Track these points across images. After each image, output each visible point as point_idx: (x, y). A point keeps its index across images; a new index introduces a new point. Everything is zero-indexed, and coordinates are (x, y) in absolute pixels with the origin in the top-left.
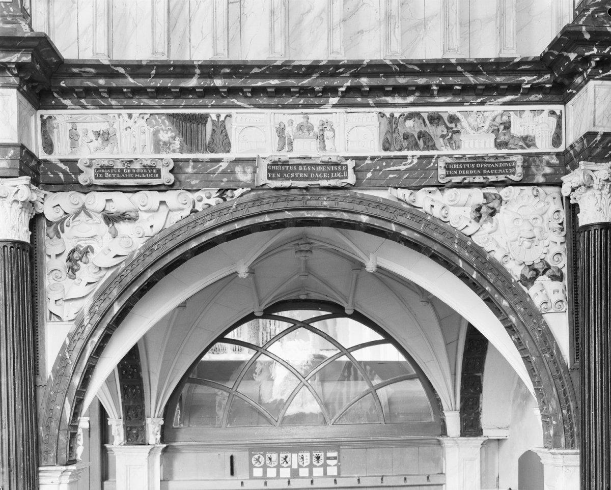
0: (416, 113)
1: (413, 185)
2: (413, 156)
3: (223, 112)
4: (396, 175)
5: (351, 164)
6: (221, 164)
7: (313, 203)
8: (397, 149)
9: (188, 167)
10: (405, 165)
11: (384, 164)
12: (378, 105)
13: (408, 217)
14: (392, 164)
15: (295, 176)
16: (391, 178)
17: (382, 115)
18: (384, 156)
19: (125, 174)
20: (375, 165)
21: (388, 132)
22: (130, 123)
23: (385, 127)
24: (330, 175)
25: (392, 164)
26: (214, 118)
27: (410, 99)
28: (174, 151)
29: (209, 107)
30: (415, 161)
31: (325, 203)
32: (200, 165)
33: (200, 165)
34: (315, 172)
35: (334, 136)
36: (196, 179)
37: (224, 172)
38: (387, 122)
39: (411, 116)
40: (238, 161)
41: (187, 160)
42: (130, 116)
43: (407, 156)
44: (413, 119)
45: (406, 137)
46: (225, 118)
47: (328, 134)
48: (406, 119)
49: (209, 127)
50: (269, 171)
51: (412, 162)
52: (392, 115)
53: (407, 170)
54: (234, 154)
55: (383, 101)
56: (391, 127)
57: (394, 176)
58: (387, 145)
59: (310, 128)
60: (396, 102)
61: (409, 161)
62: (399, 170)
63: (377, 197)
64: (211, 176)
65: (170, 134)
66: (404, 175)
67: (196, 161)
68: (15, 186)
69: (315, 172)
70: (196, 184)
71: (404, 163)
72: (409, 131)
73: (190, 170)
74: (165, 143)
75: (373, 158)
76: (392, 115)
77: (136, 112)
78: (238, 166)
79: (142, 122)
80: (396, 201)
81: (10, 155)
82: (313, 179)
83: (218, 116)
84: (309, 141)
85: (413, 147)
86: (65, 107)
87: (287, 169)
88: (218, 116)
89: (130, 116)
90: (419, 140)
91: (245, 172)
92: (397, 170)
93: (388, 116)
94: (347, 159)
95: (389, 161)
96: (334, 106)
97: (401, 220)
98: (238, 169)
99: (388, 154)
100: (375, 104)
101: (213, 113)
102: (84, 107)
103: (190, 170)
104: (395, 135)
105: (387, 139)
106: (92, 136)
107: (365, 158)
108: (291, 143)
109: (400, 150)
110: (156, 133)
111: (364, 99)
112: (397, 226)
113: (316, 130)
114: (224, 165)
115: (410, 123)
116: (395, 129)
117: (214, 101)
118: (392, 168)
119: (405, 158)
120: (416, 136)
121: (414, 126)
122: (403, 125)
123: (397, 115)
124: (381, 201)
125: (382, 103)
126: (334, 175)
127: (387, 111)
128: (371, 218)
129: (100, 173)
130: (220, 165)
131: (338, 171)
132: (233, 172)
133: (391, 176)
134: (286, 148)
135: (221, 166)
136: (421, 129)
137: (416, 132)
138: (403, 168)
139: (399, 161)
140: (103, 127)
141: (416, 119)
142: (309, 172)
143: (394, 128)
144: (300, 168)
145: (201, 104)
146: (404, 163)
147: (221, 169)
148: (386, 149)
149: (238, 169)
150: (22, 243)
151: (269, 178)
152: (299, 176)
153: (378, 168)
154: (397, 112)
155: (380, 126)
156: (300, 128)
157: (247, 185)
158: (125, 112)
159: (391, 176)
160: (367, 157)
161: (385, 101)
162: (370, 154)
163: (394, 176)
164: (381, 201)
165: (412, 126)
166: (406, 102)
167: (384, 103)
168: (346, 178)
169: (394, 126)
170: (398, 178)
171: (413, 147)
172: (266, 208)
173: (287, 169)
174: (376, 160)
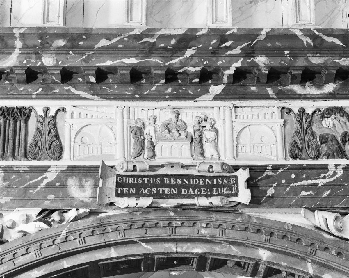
0: (337, 108)
1: (338, 206)
2: (336, 166)
3: (54, 105)
4: (311, 192)
5: (243, 175)
6: (45, 175)
7: (185, 232)
8: (312, 156)
10: (324, 178)
11: (293, 176)
12: (282, 96)
13: (333, 253)
14: (304, 176)
15: (158, 192)
16: (303, 196)
17: (285, 111)
18: (292, 165)
20: (281, 176)
21: (297, 133)
23: (293, 125)
24: (212, 191)
25: (304, 176)
26: (41, 113)
27: (329, 88)
29: (34, 96)
30: (340, 172)
31: (203, 231)
32: (14, 176)
33: (14, 176)
34: (188, 187)
35: (217, 138)
36: (7, 196)
37: (50, 186)
38: (295, 120)
39: (330, 111)
40: (73, 170)
43: (327, 165)
44: (333, 117)
45: (324, 139)
46: (57, 113)
47: (208, 135)
48: (323, 117)
49: (32, 124)
50: (118, 185)
51: (335, 173)
52: (302, 111)
53: (327, 185)
54: (67, 161)
55: (289, 90)
56: (301, 126)
57: (309, 193)
58: (297, 151)
59: (182, 128)
60: (308, 93)
61: (330, 173)
62: (316, 185)
63: (284, 223)
64: (31, 191)
66: (323, 192)
69: (188, 187)
70: (6, 203)
71: (323, 175)
72: (327, 131)
75: (275, 168)
76: (302, 111)
78: (72, 178)
80: (313, 229)
82: (184, 197)
83: (47, 109)
84: (177, 145)
85: (335, 154)
87: (146, 182)
90: (344, 144)
91: (81, 186)
92: (312, 185)
93: (297, 112)
94: (236, 168)
95: (300, 172)
96: (217, 98)
97: (322, 256)
98: (72, 182)
99: (298, 162)
100: (276, 95)
104: (307, 138)
105: (296, 143)
107: (264, 168)
108: (153, 146)
109: (317, 157)
111: (261, 87)
112: (316, 266)
113: (190, 130)
114: (51, 176)
115: (328, 122)
116: (307, 129)
117: (40, 89)
118: (305, 182)
119: (325, 168)
120: (339, 139)
121: (334, 126)
122: (319, 124)
123: (309, 111)
124: (290, 228)
125: (288, 93)
126: (217, 191)
127: (295, 105)
128: (275, 254)
130: (44, 176)
131: (223, 186)
132: (64, 186)
133: (304, 193)
134: (146, 154)
135: (46, 178)
136: (346, 130)
137: (338, 133)
138: (321, 182)
139: (315, 172)
141: (338, 117)
142: (179, 187)
143: (305, 128)
144: (166, 181)
145: (22, 93)
146: (323, 175)
147: (45, 182)
148: (294, 157)
149: (72, 182)
151: (118, 195)
152: (164, 192)
153: (283, 181)
154: (310, 106)
155: (284, 125)
156: (167, 127)
157: (85, 205)
159: (304, 193)
160: (268, 166)
161: (292, 90)
162: (271, 163)
163: (309, 193)
164: (290, 228)
165: (332, 125)
166: (322, 92)
167: (290, 93)
168: (236, 195)
169: (305, 125)
170: (315, 196)
171: (335, 154)
172: (112, 237)
173: (146, 182)
174: (281, 170)
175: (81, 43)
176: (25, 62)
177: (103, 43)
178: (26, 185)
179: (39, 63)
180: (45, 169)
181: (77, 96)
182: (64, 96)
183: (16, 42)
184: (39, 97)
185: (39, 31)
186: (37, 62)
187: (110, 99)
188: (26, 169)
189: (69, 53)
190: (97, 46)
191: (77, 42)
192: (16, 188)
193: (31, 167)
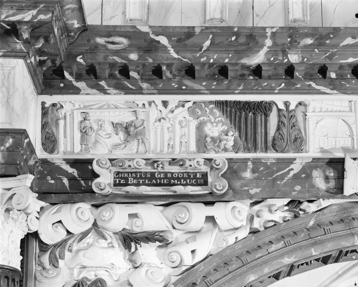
3: (294, 99)
6: (292, 166)
9: (245, 170)
19: (156, 179)
22: (165, 111)
26: (282, 106)
28: (225, 150)
29: (276, 91)
32: (262, 168)
33: (262, 168)
36: (257, 187)
40: (316, 163)
41: (245, 161)
42: (165, 104)
46: (297, 106)
64: (278, 182)
65: (221, 128)
67: (256, 162)
68: (9, 189)
70: (256, 193)
73: (248, 175)
74: (213, 139)
77: (173, 99)
78: (317, 170)
79: (182, 113)
81: (7, 145)
86: (77, 91)
88: (287, 104)
89: (165, 104)
101: (279, 100)
102: (103, 91)
103: (248, 175)
106: (109, 129)
110: (200, 128)
114: (296, 167)
117: (283, 85)
129: (122, 178)
130: (290, 168)
132: (309, 177)
135: (292, 169)
140: (126, 117)
145: (266, 88)
147: (292, 173)
150: (14, 271)
158: (158, 99)
175: (328, 42)
176: (272, 59)
177: (349, 41)
178: (274, 176)
179: (286, 60)
180: (291, 161)
181: (318, 91)
182: (305, 91)
183: (266, 41)
184: (281, 92)
185: (290, 31)
186: (283, 59)
187: (348, 93)
188: (274, 161)
189: (314, 51)
190: (341, 45)
191: (324, 40)
192: (264, 179)
193: (278, 159)
